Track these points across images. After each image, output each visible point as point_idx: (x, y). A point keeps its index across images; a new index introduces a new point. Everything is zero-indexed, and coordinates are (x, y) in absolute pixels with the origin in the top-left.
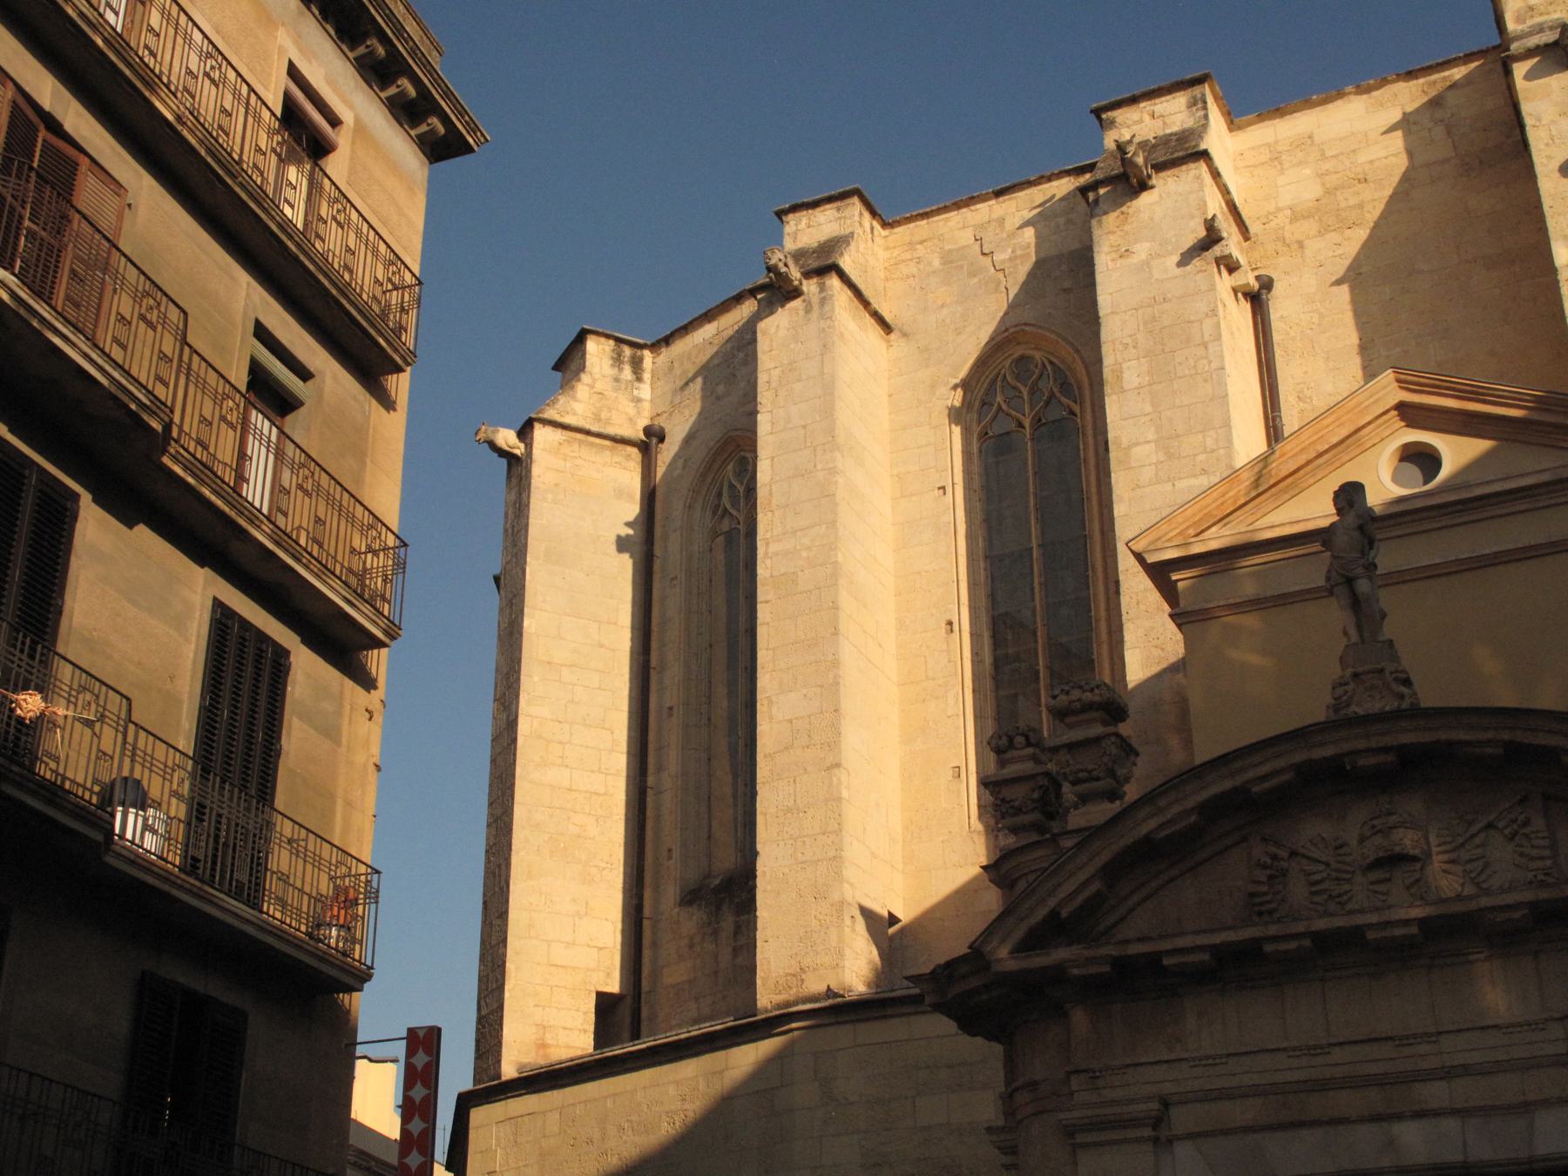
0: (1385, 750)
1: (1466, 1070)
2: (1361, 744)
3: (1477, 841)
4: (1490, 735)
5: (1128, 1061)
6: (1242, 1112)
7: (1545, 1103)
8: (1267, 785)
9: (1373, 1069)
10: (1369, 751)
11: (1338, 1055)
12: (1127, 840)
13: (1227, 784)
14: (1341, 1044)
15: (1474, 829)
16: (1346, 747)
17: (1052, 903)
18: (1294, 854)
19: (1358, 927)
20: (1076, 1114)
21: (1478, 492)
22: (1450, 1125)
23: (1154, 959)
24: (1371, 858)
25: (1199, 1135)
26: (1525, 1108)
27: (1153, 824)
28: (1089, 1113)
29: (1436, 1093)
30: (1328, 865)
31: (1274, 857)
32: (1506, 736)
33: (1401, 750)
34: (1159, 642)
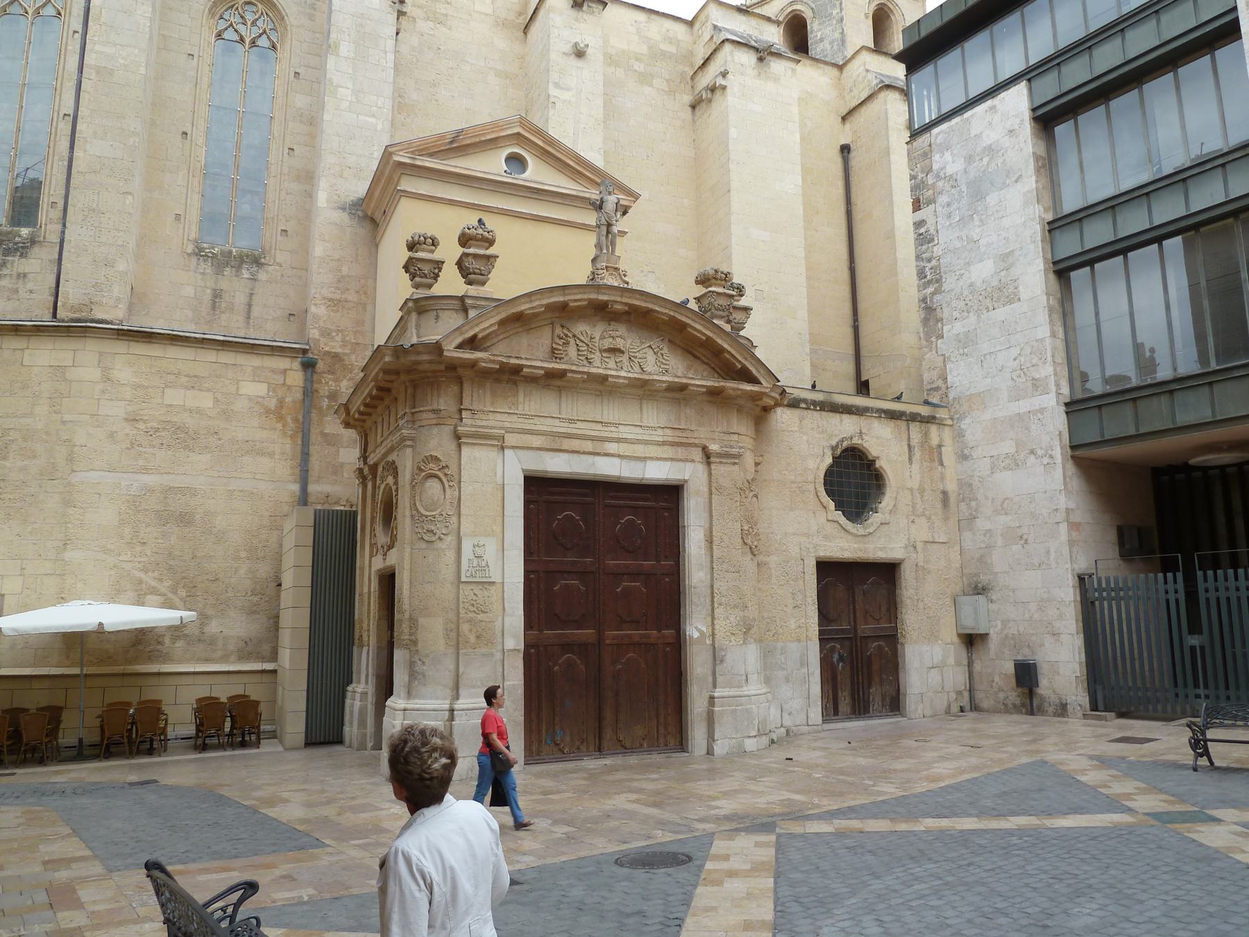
0: (626, 304)
1: (625, 441)
2: (619, 299)
3: (644, 351)
4: (667, 311)
5: (492, 410)
6: (537, 441)
7: (651, 458)
8: (576, 304)
9: (592, 433)
10: (622, 303)
11: (579, 425)
12: (514, 310)
13: (561, 299)
14: (582, 421)
15: (643, 347)
16: (612, 298)
17: (477, 330)
18: (574, 336)
19: (607, 375)
20: (466, 429)
21: (546, 188)
22: (617, 461)
23: (605, 378)
24: (606, 347)
25: (517, 447)
26: (644, 459)
27: (527, 306)
28: (473, 429)
29: (612, 447)
30: (588, 346)
31: (567, 336)
32: (672, 313)
33: (630, 305)
34: (338, 192)
